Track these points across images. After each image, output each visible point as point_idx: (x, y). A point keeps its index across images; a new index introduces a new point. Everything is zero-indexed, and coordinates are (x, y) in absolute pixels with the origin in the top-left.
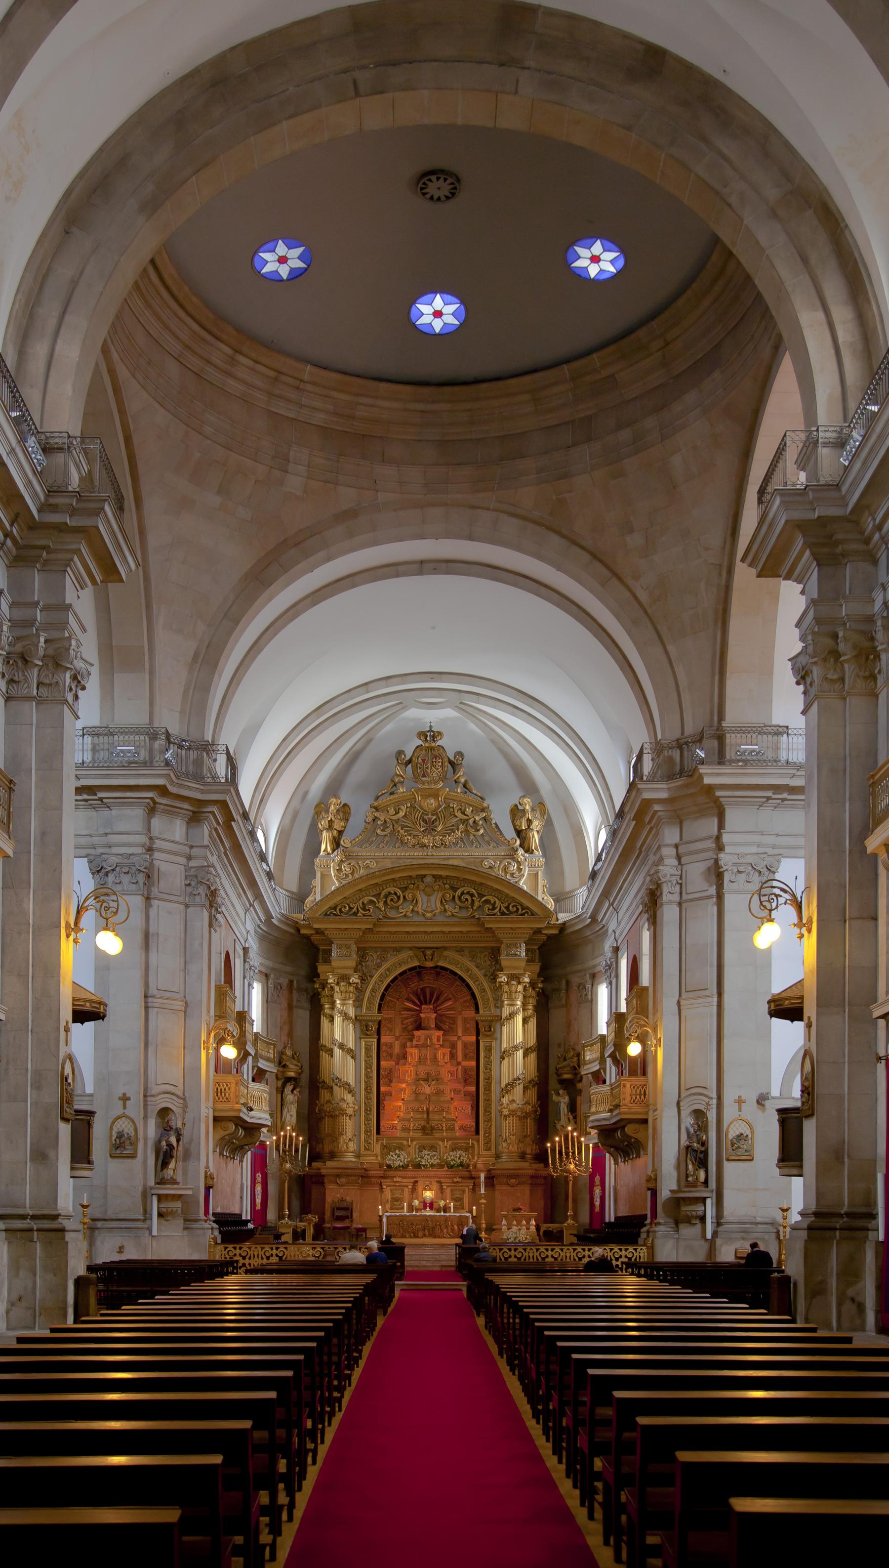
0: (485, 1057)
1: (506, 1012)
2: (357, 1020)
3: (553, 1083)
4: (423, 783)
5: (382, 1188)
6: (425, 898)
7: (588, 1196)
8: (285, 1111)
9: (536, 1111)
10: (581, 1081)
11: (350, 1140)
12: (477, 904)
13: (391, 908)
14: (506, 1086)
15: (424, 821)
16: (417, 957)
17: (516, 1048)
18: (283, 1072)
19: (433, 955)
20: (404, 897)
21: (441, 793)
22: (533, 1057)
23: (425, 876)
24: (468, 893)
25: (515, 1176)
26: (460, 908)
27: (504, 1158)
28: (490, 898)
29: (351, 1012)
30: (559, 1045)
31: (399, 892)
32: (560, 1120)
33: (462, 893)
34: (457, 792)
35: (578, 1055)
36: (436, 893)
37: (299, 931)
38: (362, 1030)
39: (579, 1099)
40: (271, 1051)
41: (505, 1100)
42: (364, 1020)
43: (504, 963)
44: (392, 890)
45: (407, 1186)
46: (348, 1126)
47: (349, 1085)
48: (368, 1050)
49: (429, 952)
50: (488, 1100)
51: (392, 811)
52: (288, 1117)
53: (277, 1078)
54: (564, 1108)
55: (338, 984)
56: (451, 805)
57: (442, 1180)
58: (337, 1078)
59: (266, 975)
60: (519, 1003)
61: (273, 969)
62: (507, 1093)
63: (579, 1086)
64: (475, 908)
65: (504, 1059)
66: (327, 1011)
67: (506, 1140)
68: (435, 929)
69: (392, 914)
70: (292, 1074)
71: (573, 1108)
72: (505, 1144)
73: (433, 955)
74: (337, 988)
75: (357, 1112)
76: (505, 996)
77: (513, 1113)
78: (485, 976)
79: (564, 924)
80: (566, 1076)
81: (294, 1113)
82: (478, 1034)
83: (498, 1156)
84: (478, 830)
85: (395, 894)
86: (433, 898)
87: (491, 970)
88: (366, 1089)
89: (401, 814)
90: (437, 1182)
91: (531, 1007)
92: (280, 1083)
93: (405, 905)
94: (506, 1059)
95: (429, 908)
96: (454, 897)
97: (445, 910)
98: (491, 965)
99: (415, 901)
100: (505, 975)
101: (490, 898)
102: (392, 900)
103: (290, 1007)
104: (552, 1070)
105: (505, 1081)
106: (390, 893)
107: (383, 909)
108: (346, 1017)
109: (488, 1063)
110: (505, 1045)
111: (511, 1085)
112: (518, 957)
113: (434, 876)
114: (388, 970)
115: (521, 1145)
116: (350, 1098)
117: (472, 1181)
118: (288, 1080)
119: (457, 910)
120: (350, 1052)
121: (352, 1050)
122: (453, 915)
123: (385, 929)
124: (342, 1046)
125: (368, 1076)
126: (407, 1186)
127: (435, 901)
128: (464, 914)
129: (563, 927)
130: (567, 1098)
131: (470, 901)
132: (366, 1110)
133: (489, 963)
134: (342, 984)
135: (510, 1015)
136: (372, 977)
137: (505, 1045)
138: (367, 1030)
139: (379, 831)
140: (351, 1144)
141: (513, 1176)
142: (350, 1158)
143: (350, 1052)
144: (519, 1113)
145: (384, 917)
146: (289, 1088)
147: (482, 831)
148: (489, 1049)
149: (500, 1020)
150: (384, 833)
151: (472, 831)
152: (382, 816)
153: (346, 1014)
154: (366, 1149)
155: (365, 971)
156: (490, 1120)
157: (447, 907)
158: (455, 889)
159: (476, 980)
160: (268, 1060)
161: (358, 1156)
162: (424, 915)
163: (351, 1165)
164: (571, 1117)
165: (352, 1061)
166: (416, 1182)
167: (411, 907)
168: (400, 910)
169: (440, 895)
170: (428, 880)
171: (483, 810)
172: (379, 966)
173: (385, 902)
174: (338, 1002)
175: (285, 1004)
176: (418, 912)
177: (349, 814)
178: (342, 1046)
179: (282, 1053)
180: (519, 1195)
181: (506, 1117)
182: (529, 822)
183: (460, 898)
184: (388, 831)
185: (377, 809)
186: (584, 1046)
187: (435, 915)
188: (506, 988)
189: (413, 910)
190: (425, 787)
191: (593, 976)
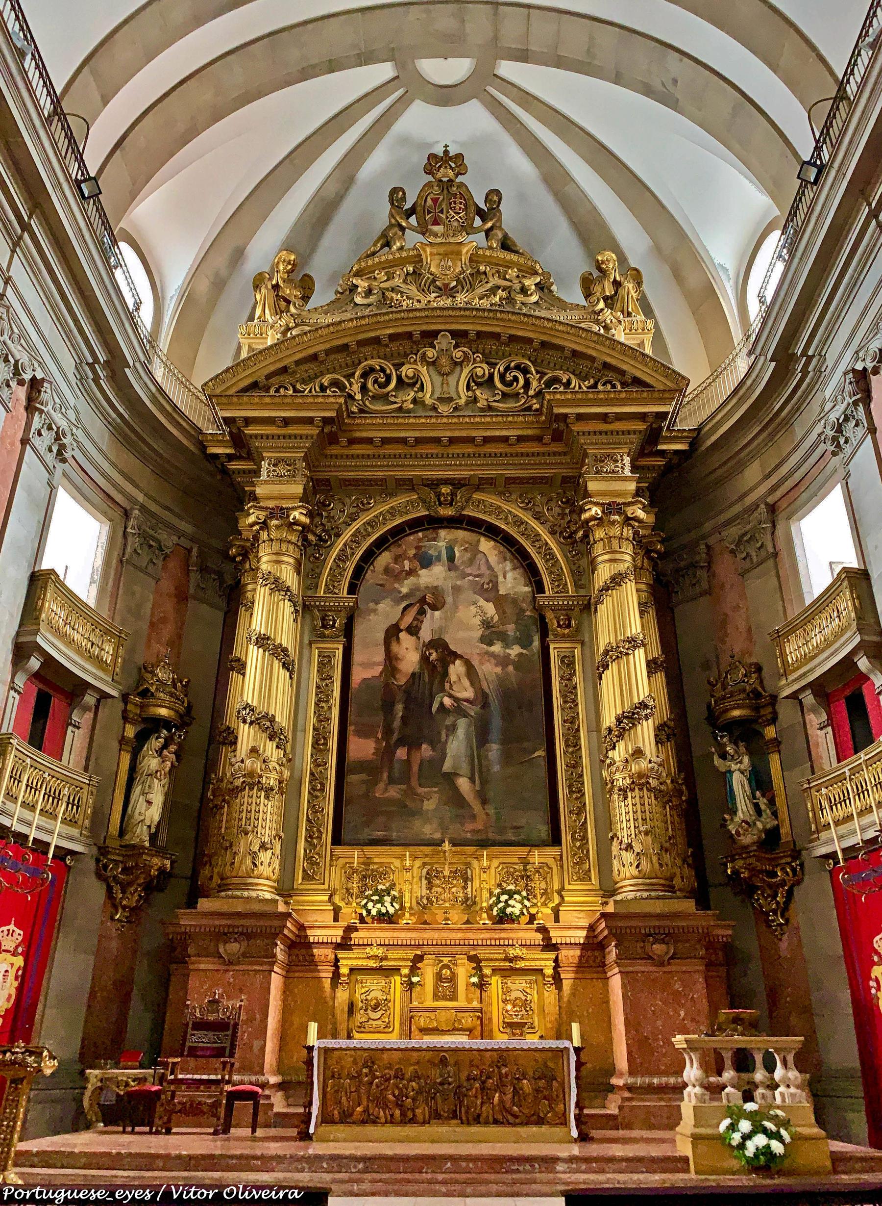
0: (562, 678)
1: (603, 573)
2: (305, 608)
3: (700, 742)
4: (436, 235)
5: (336, 975)
6: (438, 379)
7: (845, 996)
8: (137, 790)
9: (681, 793)
10: (774, 720)
11: (263, 847)
12: (534, 384)
13: (374, 397)
14: (619, 720)
15: (437, 287)
16: (424, 502)
17: (633, 643)
18: (142, 707)
19: (453, 494)
20: (399, 378)
21: (464, 251)
22: (660, 678)
23: (435, 334)
24: (518, 367)
25: (666, 936)
26: (504, 395)
27: (628, 891)
28: (559, 373)
29: (289, 576)
30: (706, 666)
31: (390, 368)
32: (734, 812)
33: (508, 368)
34: (490, 248)
35: (759, 669)
36: (458, 369)
37: (203, 448)
38: (314, 629)
39: (775, 761)
40: (109, 648)
41: (619, 754)
42: (324, 610)
43: (592, 486)
44: (375, 363)
45: (397, 970)
46: (266, 815)
47: (272, 720)
48: (325, 663)
49: (445, 490)
50: (575, 765)
51: (382, 276)
52: (141, 805)
53: (125, 718)
54: (739, 783)
55: (265, 525)
56: (482, 268)
57: (481, 953)
58: (247, 706)
59: (126, 514)
60: (628, 558)
61: (143, 508)
62: (620, 736)
63: (770, 732)
64: (531, 393)
65: (606, 667)
66: (249, 595)
67: (629, 847)
68: (457, 434)
69: (378, 407)
70: (163, 712)
71: (760, 781)
72: (628, 857)
73: (453, 494)
74: (264, 535)
75: (288, 789)
76: (598, 549)
77: (639, 782)
78: (552, 533)
79: (699, 430)
80: (736, 713)
81: (158, 797)
82: (544, 632)
83: (609, 891)
84: (531, 295)
85: (383, 370)
86: (452, 380)
87: (564, 523)
88: (315, 743)
89: (397, 281)
90: (471, 959)
91: (643, 587)
92: (130, 731)
93: (400, 394)
94: (613, 667)
95: (444, 387)
96: (491, 376)
97: (475, 400)
98: (562, 515)
99: (415, 382)
100: (596, 504)
101: (559, 373)
102: (375, 381)
103: (182, 597)
104: (696, 713)
105: (609, 719)
106: (372, 370)
107: (358, 397)
108: (277, 586)
109: (569, 692)
110: (604, 639)
111: (629, 719)
112: (615, 481)
113: (454, 334)
114: (368, 523)
115: (667, 857)
116: (271, 750)
117: (552, 955)
118: (151, 727)
119: (498, 398)
120: (279, 652)
121: (284, 650)
122: (490, 408)
123: (364, 434)
124: (263, 641)
125: (322, 719)
126: (397, 970)
127: (459, 385)
128: (510, 404)
129: (696, 437)
130: (746, 759)
131: (521, 382)
132: (313, 789)
133: (558, 510)
134: (274, 522)
135: (613, 578)
136: (338, 535)
137: (604, 639)
138: (324, 626)
139: (358, 300)
140: (265, 856)
141: (663, 930)
142: (264, 891)
143: (279, 652)
144: (653, 783)
145: (361, 411)
146: (155, 743)
147: (534, 298)
148: (568, 662)
149: (588, 607)
150: (365, 301)
151: (520, 298)
152: (362, 284)
153: (277, 580)
154: (307, 877)
155: (328, 526)
156: (582, 809)
157: (478, 392)
158: (493, 365)
159: (537, 537)
160: (98, 661)
161: (285, 890)
162: (434, 408)
163: (256, 907)
164: (763, 803)
165: (284, 674)
166: (419, 958)
167: (412, 394)
168: (393, 399)
169: (466, 371)
170: (444, 342)
171: (536, 273)
172: (353, 518)
173: (364, 389)
174: (264, 559)
175: (167, 586)
176: (423, 403)
177: (312, 290)
178: (263, 641)
179: (146, 669)
180: (678, 986)
181: (623, 791)
182: (617, 284)
183: (502, 377)
184: (371, 299)
185: (357, 275)
186: (780, 637)
187: (456, 409)
188: (599, 534)
189: (414, 401)
190: (439, 240)
191: (772, 509)
